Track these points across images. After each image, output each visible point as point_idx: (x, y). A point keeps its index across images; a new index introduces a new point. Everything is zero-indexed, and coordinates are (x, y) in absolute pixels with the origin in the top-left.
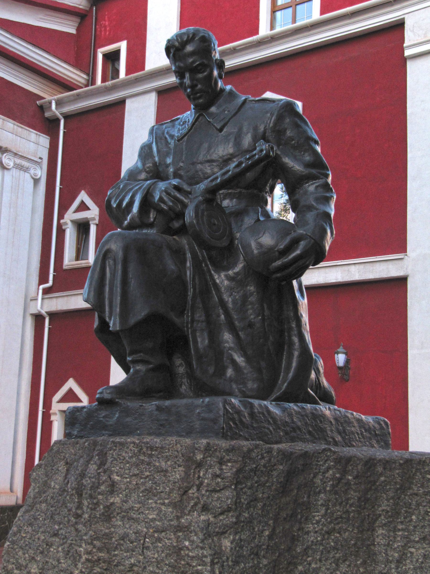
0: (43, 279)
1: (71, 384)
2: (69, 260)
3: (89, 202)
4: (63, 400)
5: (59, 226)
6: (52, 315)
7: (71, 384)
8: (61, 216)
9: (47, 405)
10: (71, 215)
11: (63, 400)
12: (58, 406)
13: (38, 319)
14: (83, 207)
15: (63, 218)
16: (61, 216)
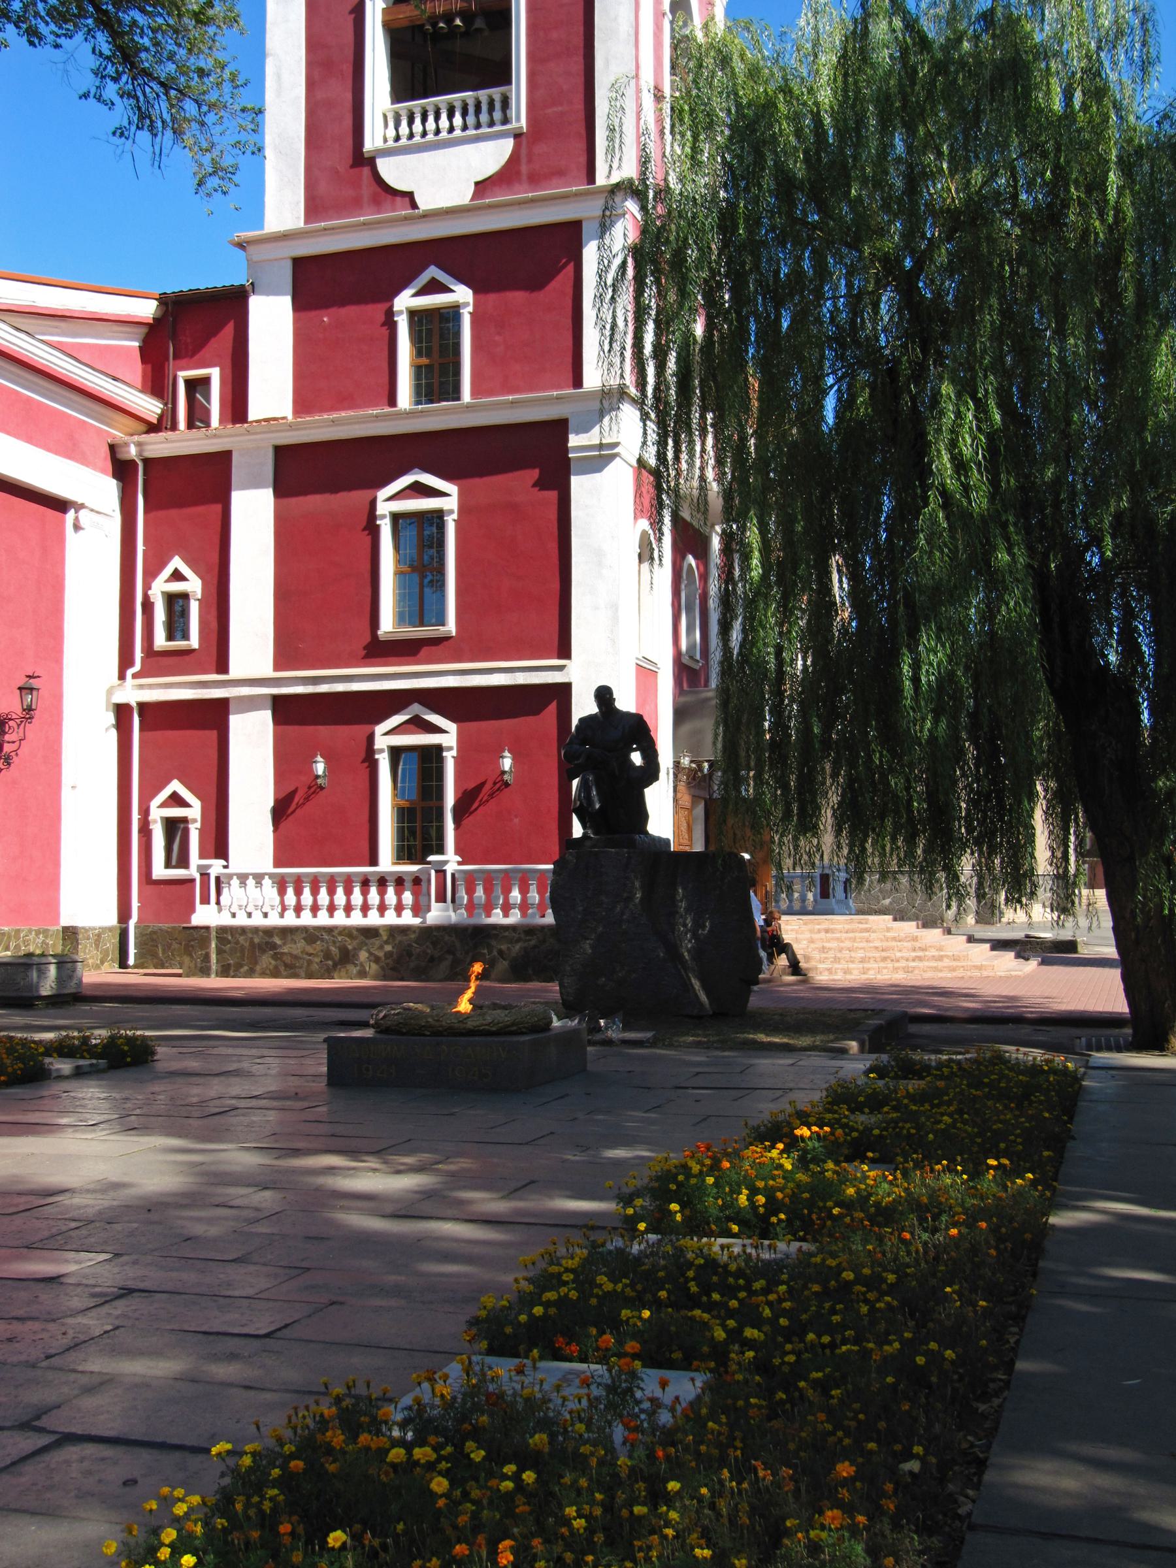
0: (125, 660)
1: (175, 786)
2: (160, 640)
3: (185, 570)
4: (163, 805)
5: (146, 597)
6: (142, 706)
7: (175, 786)
8: (147, 587)
9: (145, 812)
10: (161, 586)
11: (163, 805)
12: (158, 813)
13: (122, 712)
14: (177, 576)
15: (150, 588)
16: (147, 587)
